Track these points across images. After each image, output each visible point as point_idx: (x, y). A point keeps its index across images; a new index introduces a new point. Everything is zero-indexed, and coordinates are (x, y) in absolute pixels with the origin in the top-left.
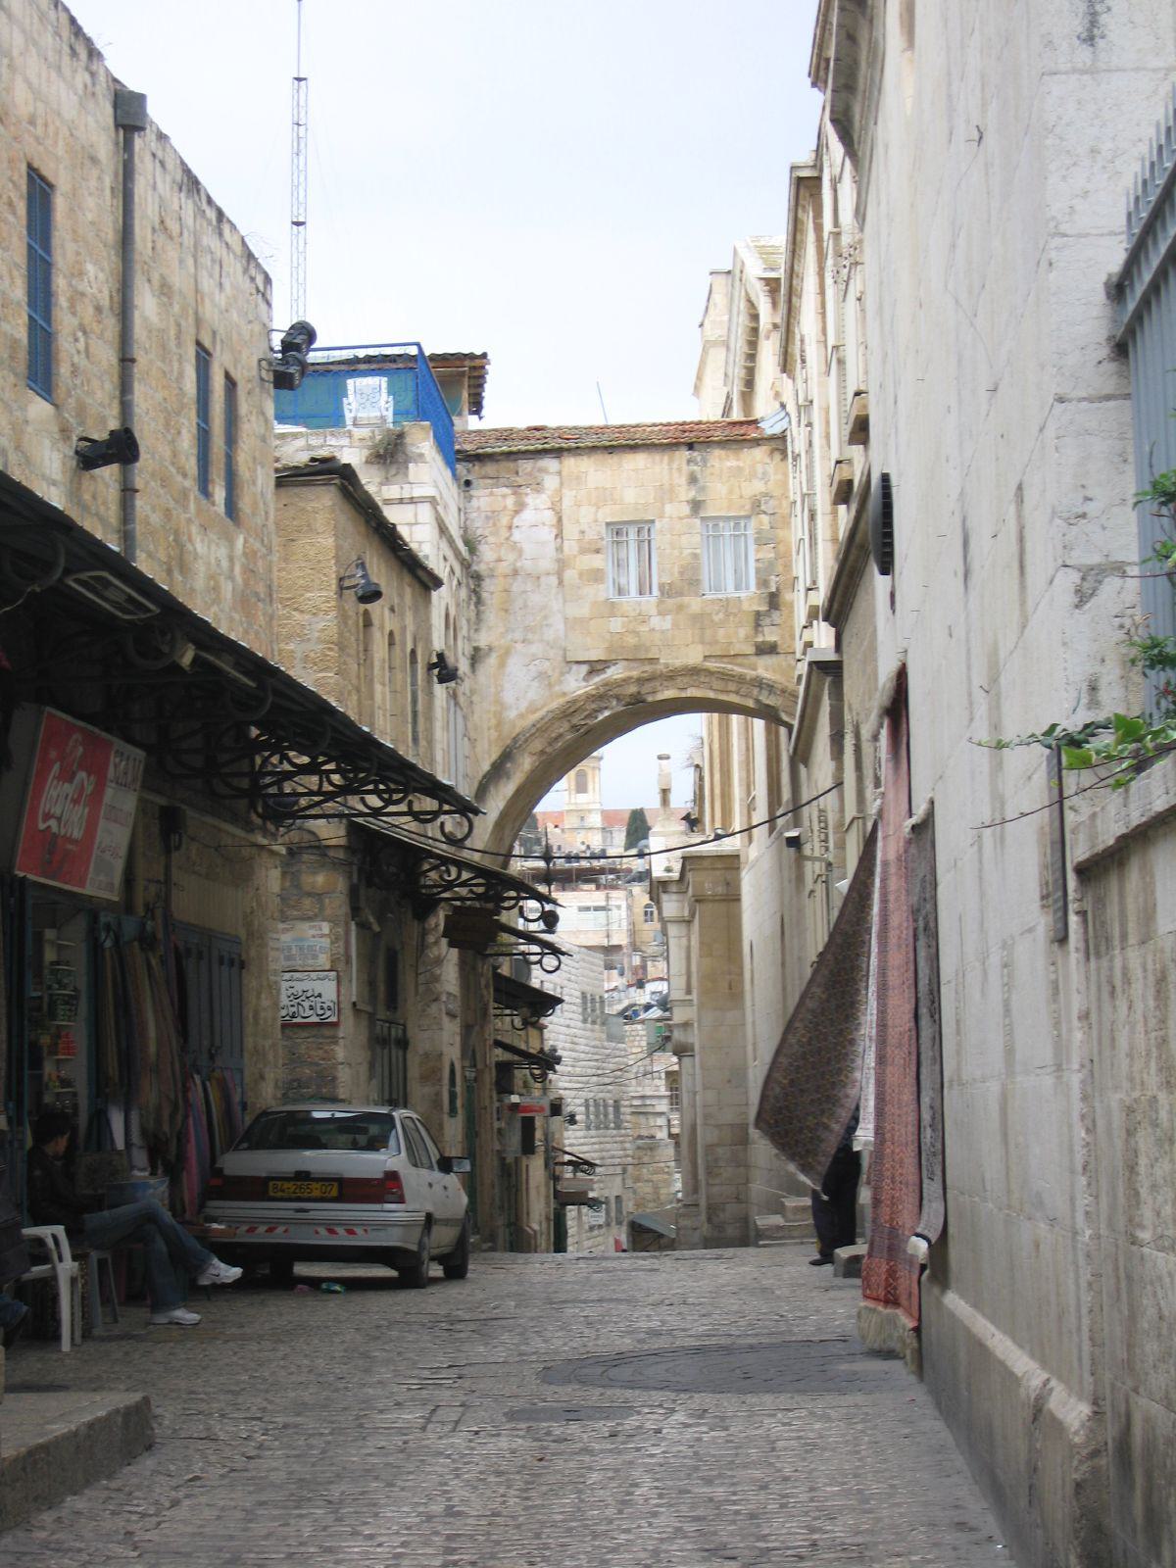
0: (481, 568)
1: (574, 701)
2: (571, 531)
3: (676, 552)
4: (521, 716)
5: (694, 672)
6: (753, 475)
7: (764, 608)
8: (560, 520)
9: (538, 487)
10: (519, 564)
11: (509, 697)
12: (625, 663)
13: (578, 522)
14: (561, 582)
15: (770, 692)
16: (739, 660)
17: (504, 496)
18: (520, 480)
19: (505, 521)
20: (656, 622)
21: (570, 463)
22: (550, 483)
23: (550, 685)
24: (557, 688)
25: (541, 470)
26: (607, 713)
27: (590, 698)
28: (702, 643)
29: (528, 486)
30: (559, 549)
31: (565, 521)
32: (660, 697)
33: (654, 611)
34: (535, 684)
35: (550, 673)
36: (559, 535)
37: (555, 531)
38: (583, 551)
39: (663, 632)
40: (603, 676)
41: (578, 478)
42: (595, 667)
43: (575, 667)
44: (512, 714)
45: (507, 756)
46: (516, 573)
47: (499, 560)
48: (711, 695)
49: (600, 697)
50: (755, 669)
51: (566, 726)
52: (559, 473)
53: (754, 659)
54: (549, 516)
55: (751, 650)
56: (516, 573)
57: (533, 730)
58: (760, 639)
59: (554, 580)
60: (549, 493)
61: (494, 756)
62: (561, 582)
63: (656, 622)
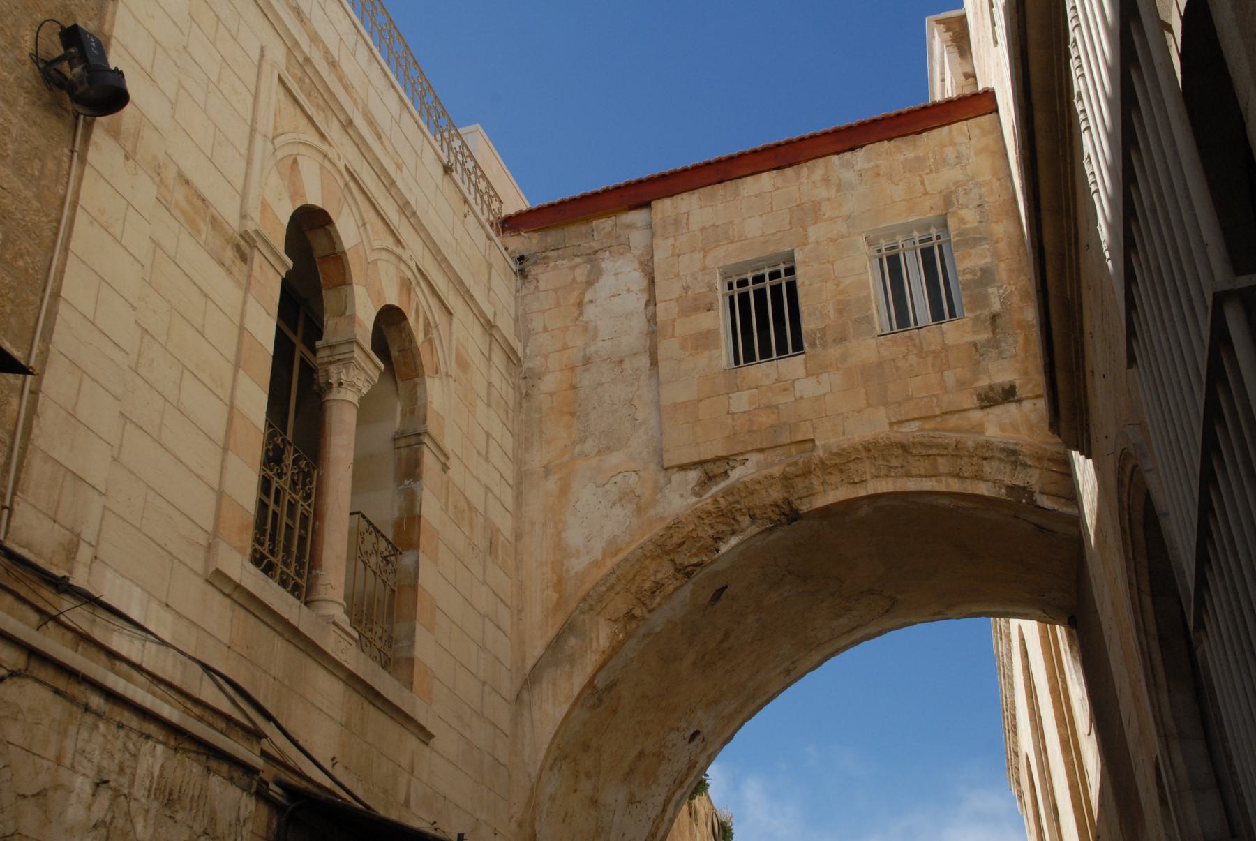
0: (537, 363)
1: (677, 524)
2: (668, 291)
3: (830, 285)
4: (596, 564)
5: (876, 450)
6: (944, 162)
7: (984, 336)
8: (652, 282)
9: (626, 246)
10: (592, 349)
11: (574, 537)
12: (760, 456)
13: (677, 275)
14: (654, 362)
15: (1015, 464)
16: (953, 421)
17: (573, 268)
18: (596, 246)
19: (573, 298)
20: (807, 387)
21: (665, 207)
22: (638, 239)
23: (639, 510)
24: (652, 512)
25: (630, 226)
26: (733, 541)
27: (701, 515)
28: (885, 405)
29: (604, 249)
30: (652, 320)
31: (656, 275)
32: (820, 502)
33: (801, 372)
34: (618, 511)
35: (638, 491)
36: (651, 301)
37: (644, 297)
38: (686, 312)
39: (817, 398)
40: (723, 484)
41: (677, 222)
42: (710, 470)
43: (676, 477)
44: (577, 565)
45: (568, 628)
46: (587, 361)
47: (565, 347)
48: (912, 485)
49: (725, 517)
50: (979, 429)
51: (666, 570)
52: (650, 225)
53: (977, 415)
54: (636, 279)
55: (969, 400)
56: (587, 361)
57: (612, 580)
58: (984, 382)
59: (645, 361)
60: (637, 252)
61: (551, 633)
62: (654, 362)
63: (807, 387)
